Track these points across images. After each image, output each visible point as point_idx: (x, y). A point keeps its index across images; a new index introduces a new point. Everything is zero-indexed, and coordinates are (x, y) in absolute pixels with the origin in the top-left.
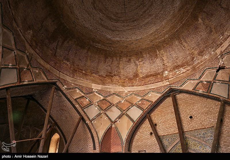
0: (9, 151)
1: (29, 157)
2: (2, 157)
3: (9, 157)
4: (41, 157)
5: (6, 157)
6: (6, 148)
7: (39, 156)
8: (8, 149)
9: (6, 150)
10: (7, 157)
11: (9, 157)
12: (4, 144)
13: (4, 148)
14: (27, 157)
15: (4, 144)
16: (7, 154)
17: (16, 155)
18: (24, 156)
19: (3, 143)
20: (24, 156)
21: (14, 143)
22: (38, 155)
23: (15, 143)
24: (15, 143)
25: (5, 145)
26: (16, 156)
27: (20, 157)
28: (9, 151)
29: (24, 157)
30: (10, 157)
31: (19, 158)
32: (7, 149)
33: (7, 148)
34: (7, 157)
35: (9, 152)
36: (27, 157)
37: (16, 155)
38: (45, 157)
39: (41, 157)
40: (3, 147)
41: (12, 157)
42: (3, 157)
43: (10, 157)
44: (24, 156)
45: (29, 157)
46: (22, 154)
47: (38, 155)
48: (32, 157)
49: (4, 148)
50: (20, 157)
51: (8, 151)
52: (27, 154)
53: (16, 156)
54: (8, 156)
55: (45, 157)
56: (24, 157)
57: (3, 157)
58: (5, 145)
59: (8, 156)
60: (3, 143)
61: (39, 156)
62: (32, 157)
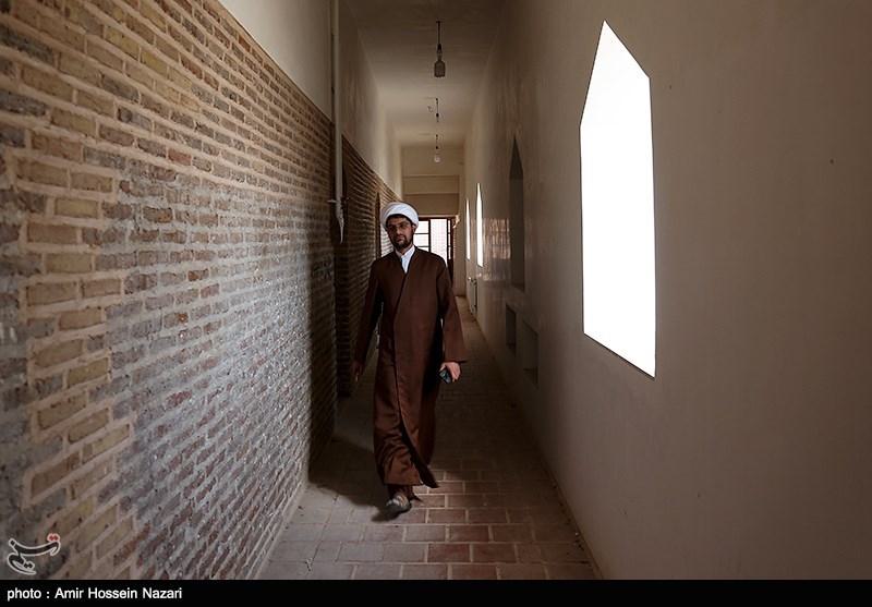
0: (35, 573)
1: (108, 594)
2: (9, 597)
3: (33, 594)
4: (156, 595)
5: (22, 595)
6: (21, 562)
7: (148, 593)
8: (31, 566)
9: (24, 568)
10: (26, 594)
11: (33, 594)
12: (17, 547)
13: (14, 562)
14: (102, 594)
15: (17, 547)
16: (24, 584)
17: (60, 589)
18: (90, 593)
19: (12, 543)
21: (51, 542)
22: (145, 590)
23: (56, 544)
24: (56, 544)
25: (20, 550)
26: (59, 592)
27: (77, 594)
28: (35, 573)
29: (93, 596)
30: (38, 594)
31: (70, 601)
32: (26, 566)
34: (26, 594)
35: (35, 576)
36: (102, 594)
37: (60, 589)
38: (172, 594)
39: (156, 595)
40: (12, 558)
41: (44, 595)
42: (12, 595)
43: (38, 594)
45: (108, 594)
47: (145, 590)
48: (123, 594)
49: (14, 562)
50: (77, 594)
51: (31, 572)
53: (59, 592)
54: (32, 591)
55: (172, 594)
56: (93, 596)
57: (12, 595)
58: (20, 550)
59: (32, 591)
60: (12, 543)
61: (148, 593)
62: (123, 594)
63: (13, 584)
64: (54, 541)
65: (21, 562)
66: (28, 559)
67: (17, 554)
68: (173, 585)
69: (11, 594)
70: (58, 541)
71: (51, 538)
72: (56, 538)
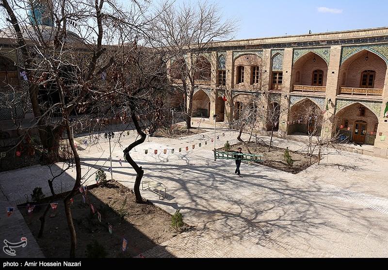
0: (15, 255)
1: (48, 264)
2: (4, 266)
3: (15, 264)
4: (69, 264)
5: (10, 264)
6: (10, 250)
7: (66, 264)
8: (14, 252)
10: (12, 264)
11: (15, 264)
12: (7, 243)
13: (6, 250)
14: (45, 264)
15: (7, 243)
16: (11, 260)
17: (26, 262)
18: (40, 264)
19: (6, 241)
20: (41, 262)
22: (64, 262)
24: (25, 242)
25: (9, 245)
26: (26, 263)
27: (34, 264)
28: (15, 255)
29: (41, 265)
30: (17, 264)
31: (31, 267)
32: (12, 252)
33: (12, 250)
34: (12, 264)
36: (45, 264)
37: (26, 262)
38: (76, 264)
39: (69, 264)
40: (5, 248)
41: (20, 264)
42: (5, 264)
43: (17, 264)
44: (41, 262)
45: (48, 264)
46: (37, 260)
47: (64, 262)
48: (55, 264)
50: (34, 264)
51: (14, 254)
52: (46, 261)
53: (26, 263)
54: (14, 263)
55: (76, 264)
56: (41, 265)
57: (5, 264)
58: (9, 245)
59: (14, 263)
60: (6, 241)
61: (66, 264)
62: (55, 264)
63: (6, 260)
64: (24, 241)
66: (12, 249)
67: (10, 247)
69: (5, 264)
70: (26, 241)
71: (23, 239)
72: (25, 239)
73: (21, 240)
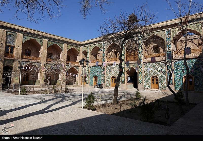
1: (25, 138)
2: (2, 139)
3: (8, 138)
4: (36, 138)
5: (5, 138)
6: (5, 130)
7: (34, 138)
8: (7, 132)
9: (5, 132)
10: (6, 138)
11: (8, 138)
12: (4, 127)
13: (3, 131)
14: (24, 138)
15: (4, 127)
17: (14, 137)
18: (21, 138)
20: (22, 137)
22: (34, 137)
23: (13, 126)
24: (13, 126)
25: (5, 128)
26: (14, 138)
27: (18, 138)
29: (22, 138)
30: (9, 138)
31: (16, 140)
32: (6, 131)
34: (6, 138)
36: (24, 138)
37: (14, 137)
38: (40, 138)
39: (36, 138)
40: (3, 130)
41: (10, 138)
43: (9, 138)
44: (22, 137)
45: (25, 138)
47: (34, 137)
48: (29, 138)
50: (18, 138)
53: (14, 138)
54: (7, 137)
55: (40, 138)
56: (22, 138)
57: (3, 138)
59: (7, 137)
61: (34, 138)
62: (29, 138)
65: (5, 130)
67: (5, 129)
68: (40, 136)
69: (3, 138)
70: (14, 126)
71: (12, 125)
73: (11, 125)
